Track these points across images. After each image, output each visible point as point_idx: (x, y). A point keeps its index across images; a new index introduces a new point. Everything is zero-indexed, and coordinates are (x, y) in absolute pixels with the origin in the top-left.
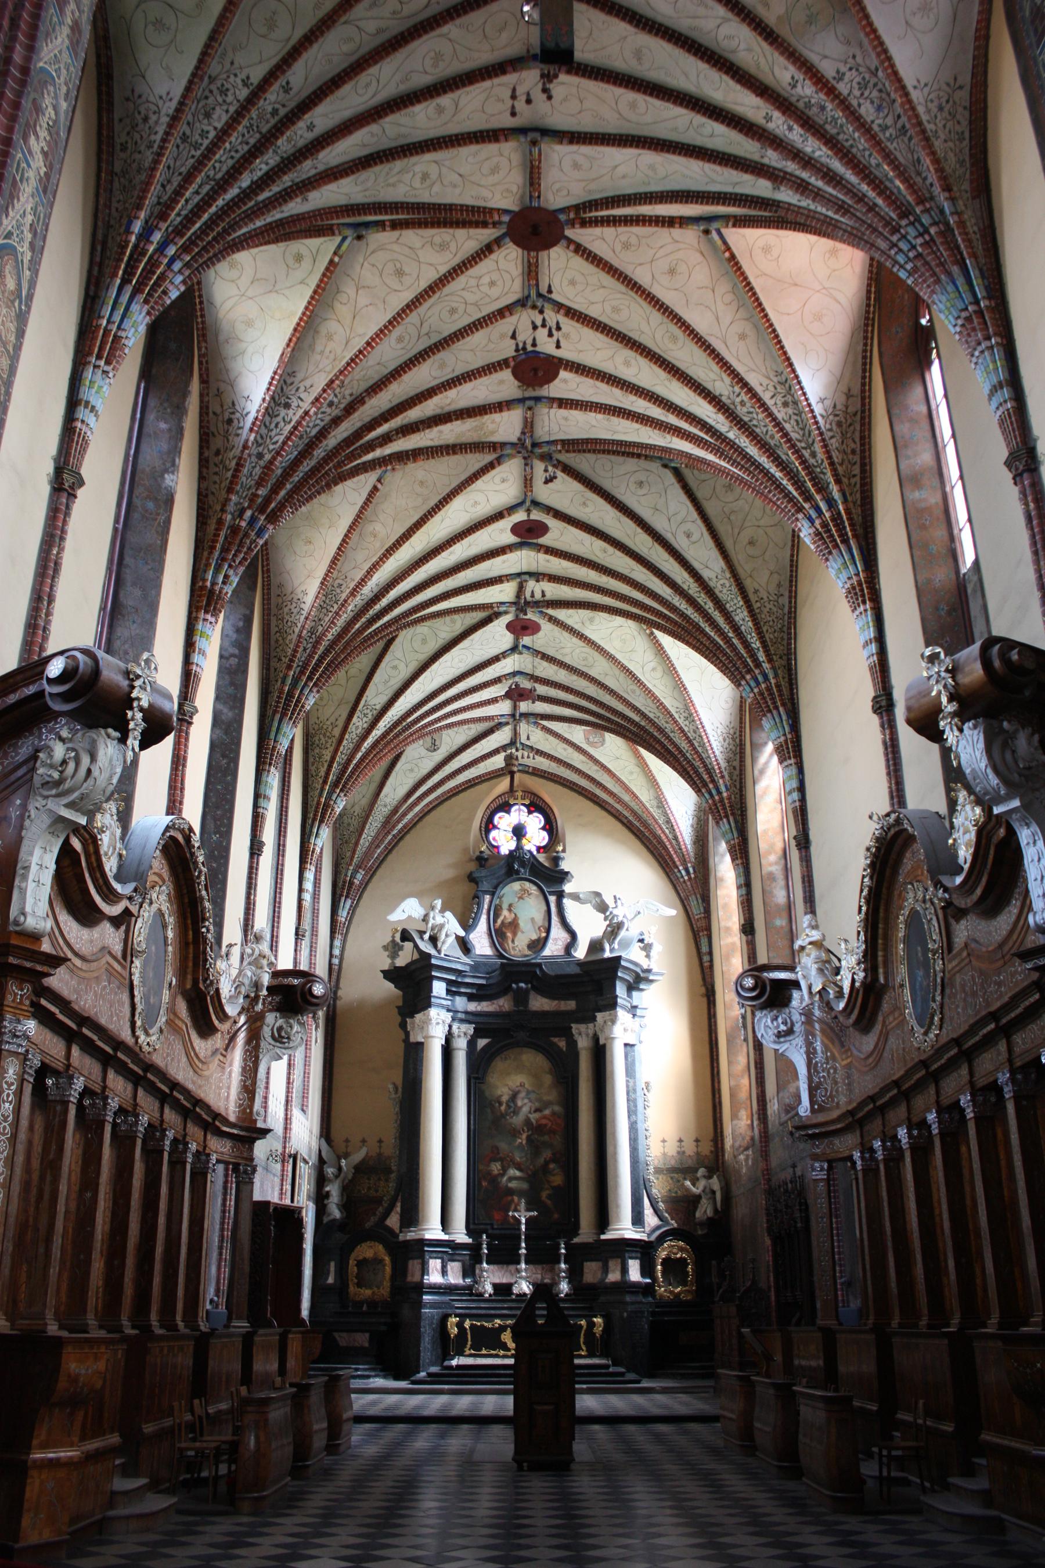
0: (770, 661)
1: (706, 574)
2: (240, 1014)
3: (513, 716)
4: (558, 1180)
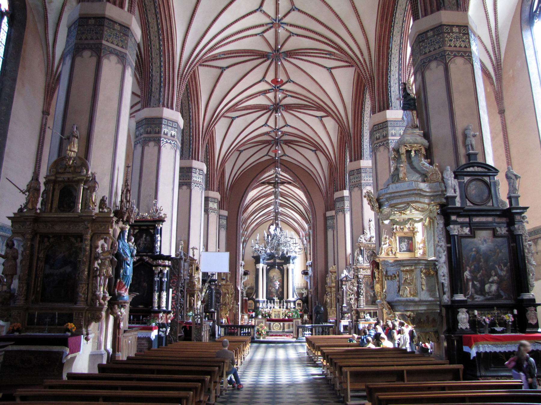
4: (281, 290)
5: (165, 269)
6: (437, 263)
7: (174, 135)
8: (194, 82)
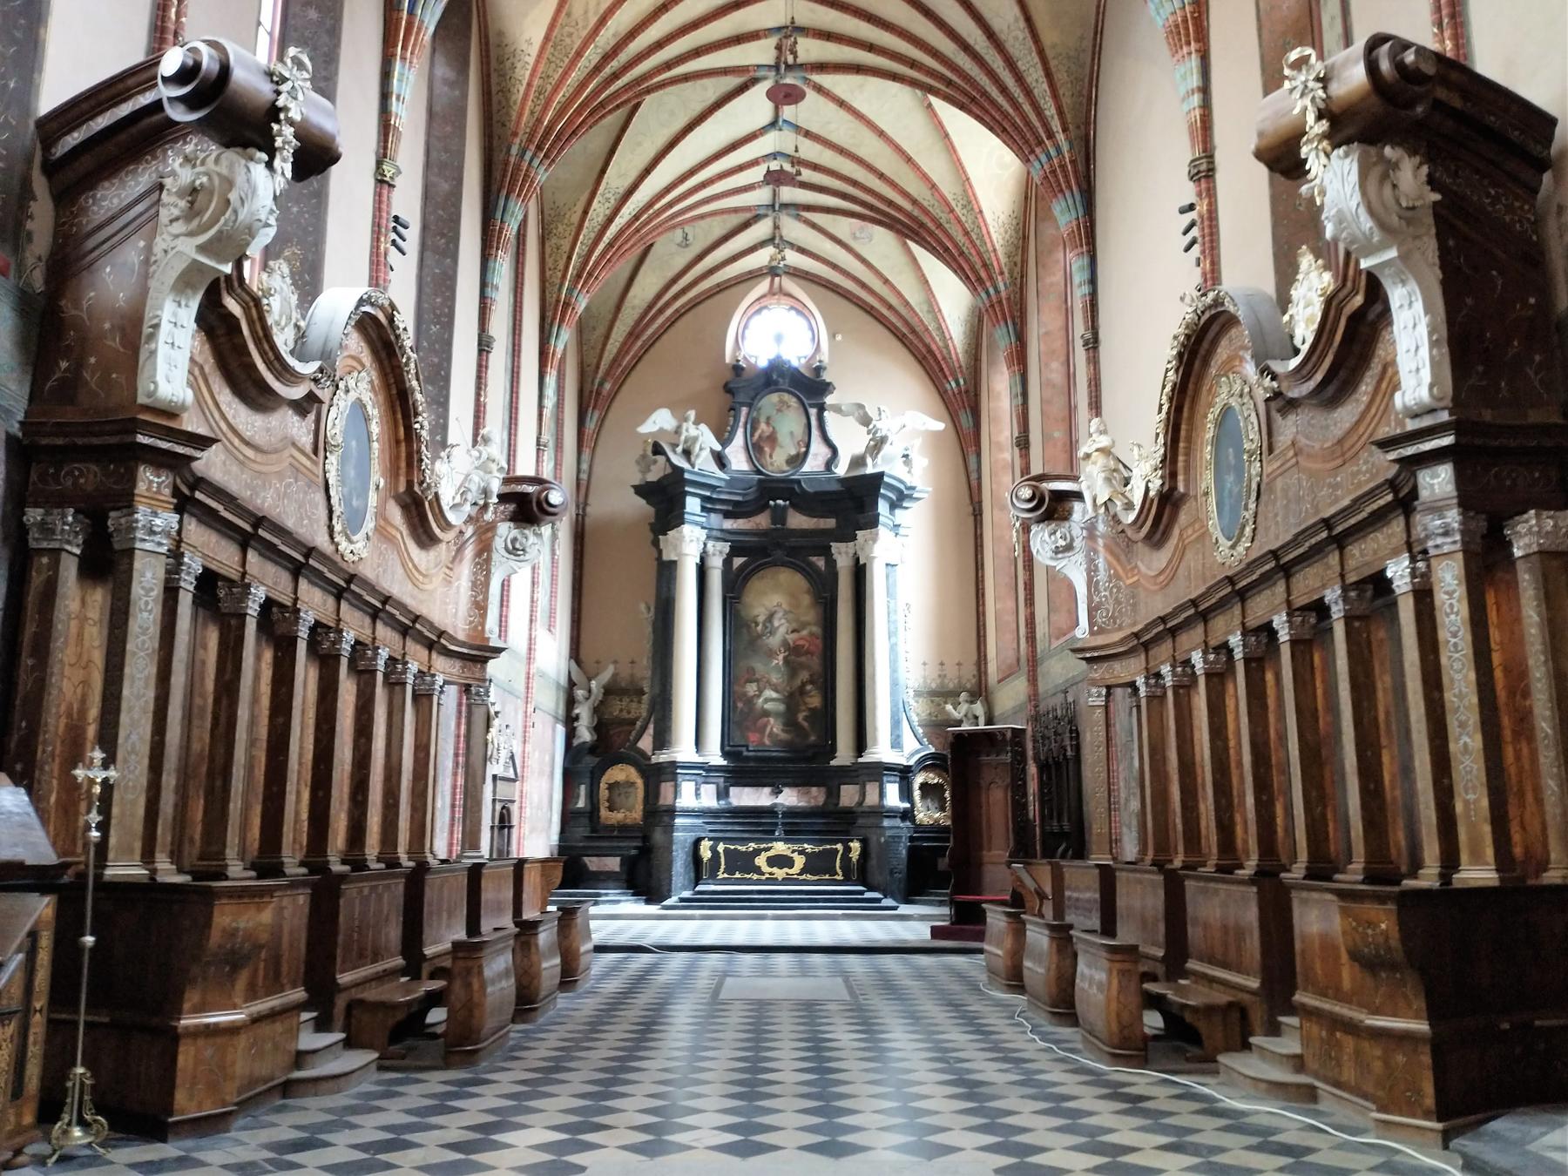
0: (1065, 130)
1: (997, 24)
2: (465, 522)
3: (773, 206)
4: (815, 701)
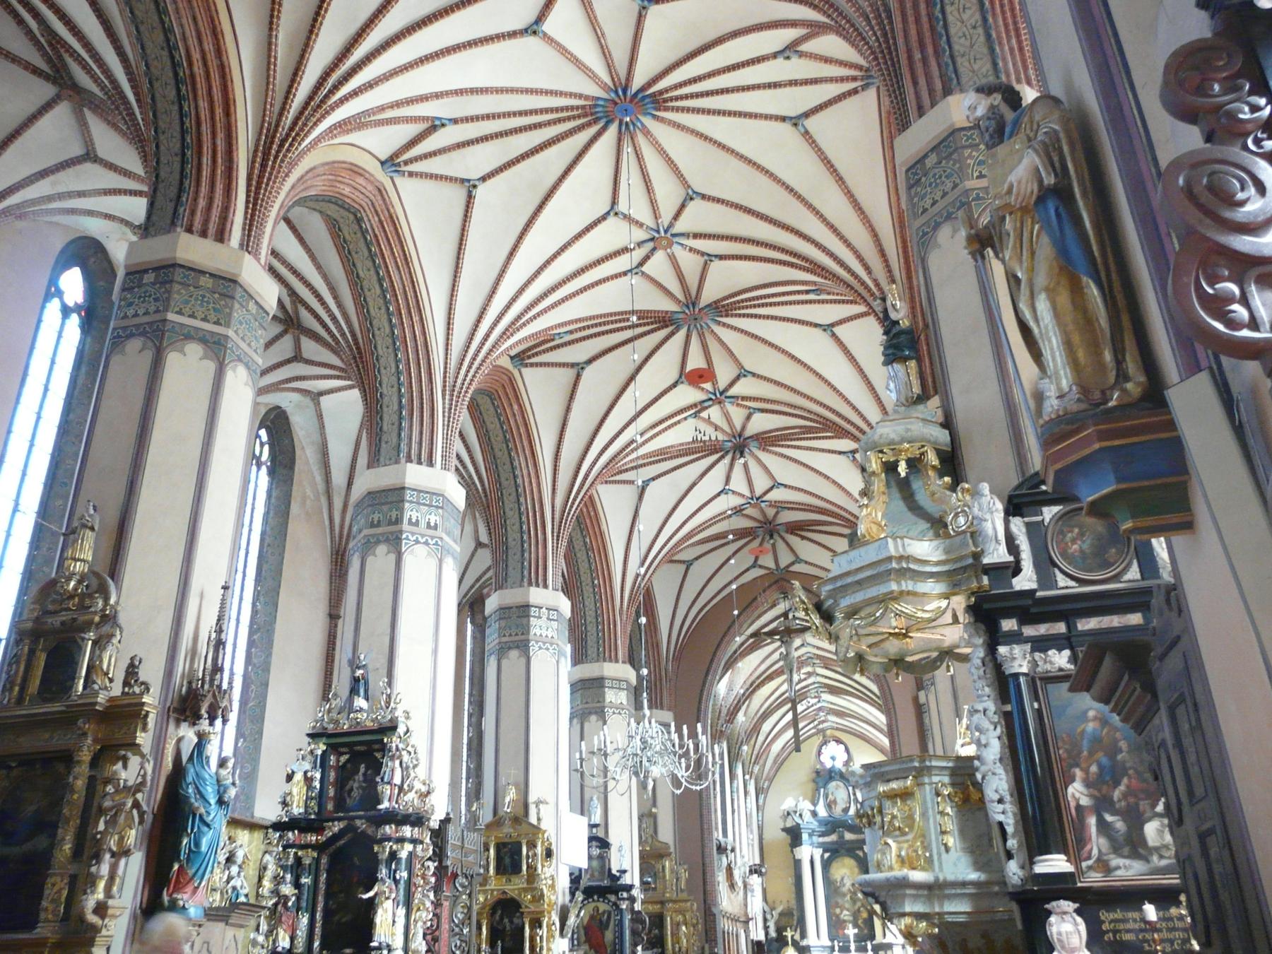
5: (403, 848)
6: (976, 763)
7: (436, 524)
8: (516, 407)
